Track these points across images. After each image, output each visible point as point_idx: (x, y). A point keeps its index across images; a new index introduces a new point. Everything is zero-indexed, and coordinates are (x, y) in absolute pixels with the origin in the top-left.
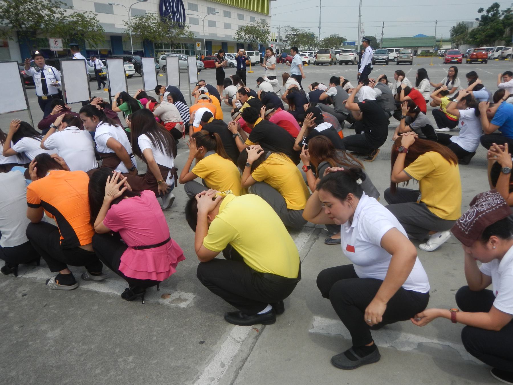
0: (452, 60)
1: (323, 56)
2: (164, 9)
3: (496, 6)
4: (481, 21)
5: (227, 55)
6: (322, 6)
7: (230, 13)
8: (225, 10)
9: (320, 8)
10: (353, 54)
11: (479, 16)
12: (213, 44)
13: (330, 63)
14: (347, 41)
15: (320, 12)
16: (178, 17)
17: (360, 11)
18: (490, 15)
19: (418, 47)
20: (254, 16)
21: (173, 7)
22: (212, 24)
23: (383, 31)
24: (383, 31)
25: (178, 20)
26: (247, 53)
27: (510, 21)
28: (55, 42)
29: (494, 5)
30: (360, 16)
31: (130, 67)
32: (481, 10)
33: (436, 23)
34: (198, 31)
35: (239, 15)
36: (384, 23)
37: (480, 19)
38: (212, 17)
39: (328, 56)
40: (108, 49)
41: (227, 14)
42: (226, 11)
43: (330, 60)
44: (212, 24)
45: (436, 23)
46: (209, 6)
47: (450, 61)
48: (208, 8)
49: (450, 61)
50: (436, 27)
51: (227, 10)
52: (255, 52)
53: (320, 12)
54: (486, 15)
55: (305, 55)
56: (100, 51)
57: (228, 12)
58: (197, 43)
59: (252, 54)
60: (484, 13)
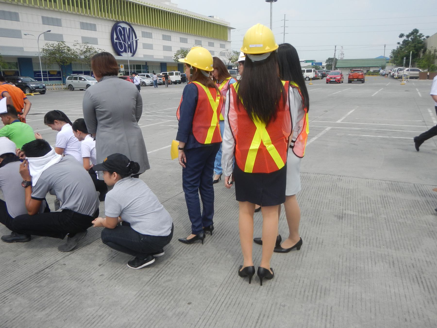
2: (115, 36)
3: (416, 31)
4: (403, 45)
5: (146, 76)
6: (285, 33)
7: (186, 39)
8: (181, 37)
9: (284, 34)
11: (401, 40)
12: (167, 65)
14: (316, 62)
15: (284, 37)
16: (129, 43)
18: (410, 39)
19: (370, 67)
20: (213, 42)
21: (124, 35)
22: (168, 49)
23: (335, 54)
24: (335, 54)
25: (130, 46)
26: (169, 73)
27: (420, 45)
29: (414, 30)
32: (401, 36)
33: (385, 46)
35: (196, 41)
36: (336, 47)
37: (401, 43)
38: (167, 43)
41: (184, 41)
42: (182, 38)
44: (168, 49)
45: (385, 46)
46: (165, 34)
47: (329, 81)
48: (163, 36)
49: (329, 81)
50: (385, 50)
51: (183, 37)
52: (174, 72)
53: (284, 37)
54: (407, 39)
56: (49, 72)
58: (121, 65)
59: (172, 74)
60: (405, 38)
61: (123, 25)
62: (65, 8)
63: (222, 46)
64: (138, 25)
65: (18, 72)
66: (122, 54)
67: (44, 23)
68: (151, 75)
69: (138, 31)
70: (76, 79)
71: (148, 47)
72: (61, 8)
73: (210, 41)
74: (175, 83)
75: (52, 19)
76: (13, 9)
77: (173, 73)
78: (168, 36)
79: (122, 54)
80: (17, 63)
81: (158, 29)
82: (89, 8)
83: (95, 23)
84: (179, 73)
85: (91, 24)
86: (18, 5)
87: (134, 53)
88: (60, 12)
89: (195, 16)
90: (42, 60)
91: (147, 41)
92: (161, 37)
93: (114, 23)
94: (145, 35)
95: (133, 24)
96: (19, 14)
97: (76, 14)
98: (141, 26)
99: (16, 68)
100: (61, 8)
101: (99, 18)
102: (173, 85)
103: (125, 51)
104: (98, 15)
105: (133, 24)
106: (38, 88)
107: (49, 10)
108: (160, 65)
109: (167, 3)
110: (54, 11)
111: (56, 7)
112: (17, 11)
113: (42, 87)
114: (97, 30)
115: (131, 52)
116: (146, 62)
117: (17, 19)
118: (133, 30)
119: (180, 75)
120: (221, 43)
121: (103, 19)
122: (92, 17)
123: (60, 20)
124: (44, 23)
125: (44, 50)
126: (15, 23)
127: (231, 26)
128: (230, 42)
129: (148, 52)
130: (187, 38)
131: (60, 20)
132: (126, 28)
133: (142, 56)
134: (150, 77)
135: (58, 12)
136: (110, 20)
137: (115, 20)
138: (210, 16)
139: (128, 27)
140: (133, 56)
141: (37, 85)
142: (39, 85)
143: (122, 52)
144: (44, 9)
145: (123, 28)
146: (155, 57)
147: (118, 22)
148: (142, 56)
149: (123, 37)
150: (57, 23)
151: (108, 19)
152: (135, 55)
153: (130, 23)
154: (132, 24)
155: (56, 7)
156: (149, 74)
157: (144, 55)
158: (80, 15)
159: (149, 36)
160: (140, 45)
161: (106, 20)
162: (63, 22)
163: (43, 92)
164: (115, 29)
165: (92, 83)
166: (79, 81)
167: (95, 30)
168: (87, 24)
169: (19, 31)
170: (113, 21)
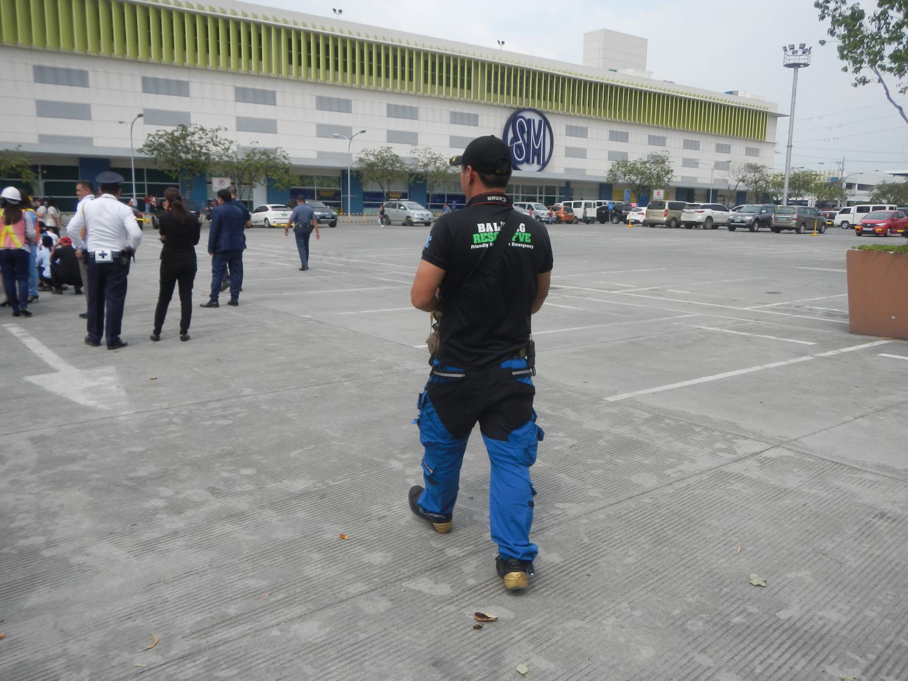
0: (864, 229)
1: (655, 213)
7: (664, 139)
8: (652, 134)
10: (702, 212)
13: (668, 225)
17: (790, 138)
21: (529, 132)
25: (537, 153)
26: (574, 203)
28: (221, 182)
30: (790, 146)
31: (283, 215)
34: (584, 168)
38: (619, 147)
39: (662, 213)
40: (404, 191)
42: (654, 137)
43: (665, 219)
48: (612, 133)
51: (656, 135)
52: (583, 202)
55: (641, 210)
57: (658, 137)
61: (528, 115)
62: (425, 90)
63: (750, 152)
64: (558, 114)
65: (340, 192)
66: (519, 166)
67: (389, 116)
68: (536, 205)
69: (558, 126)
70: (394, 206)
71: (581, 153)
72: (418, 89)
73: (720, 143)
74: (587, 220)
75: (404, 107)
76: (343, 95)
77: (581, 203)
78: (622, 133)
79: (519, 166)
80: (339, 178)
81: (601, 120)
82: (469, 87)
83: (477, 113)
84: (594, 204)
85: (469, 115)
86: (352, 88)
87: (544, 165)
88: (419, 96)
89: (697, 95)
90: (351, 176)
91: (576, 142)
92: (606, 135)
93: (512, 112)
94: (571, 131)
95: (550, 113)
96: (353, 103)
97: (445, 99)
98: (564, 115)
99: (337, 186)
100: (418, 89)
101: (485, 105)
102: (582, 226)
103: (527, 161)
104: (482, 98)
105: (550, 113)
106: (324, 217)
107: (400, 94)
108: (598, 187)
109: (630, 72)
110: (407, 95)
111: (410, 88)
112: (350, 98)
113: (330, 217)
114: (480, 124)
115: (539, 163)
116: (568, 183)
117: (348, 110)
118: (547, 123)
119: (594, 207)
120: (748, 146)
121: (492, 105)
122: (472, 103)
123: (417, 109)
124: (389, 116)
125: (361, 160)
126: (344, 115)
127: (779, 111)
128: (775, 143)
129: (576, 163)
130: (665, 136)
131: (417, 109)
132: (534, 120)
133: (562, 171)
134: (533, 209)
135: (415, 96)
136: (505, 107)
137: (515, 106)
138: (731, 93)
139: (537, 118)
140: (540, 170)
141: (324, 214)
142: (326, 213)
143: (522, 163)
144: (392, 93)
145: (529, 122)
146: (588, 173)
147: (520, 110)
148: (562, 171)
149: (525, 136)
150: (411, 114)
151: (502, 104)
152: (547, 168)
153: (544, 110)
154: (547, 112)
155: (410, 88)
156: (532, 204)
157: (567, 169)
158: (451, 100)
159: (582, 133)
160: (559, 151)
161: (499, 106)
162: (422, 113)
163: (333, 225)
164: (512, 121)
165: (414, 214)
166: (399, 210)
167: (476, 125)
168: (462, 114)
169: (350, 129)
170: (511, 108)
